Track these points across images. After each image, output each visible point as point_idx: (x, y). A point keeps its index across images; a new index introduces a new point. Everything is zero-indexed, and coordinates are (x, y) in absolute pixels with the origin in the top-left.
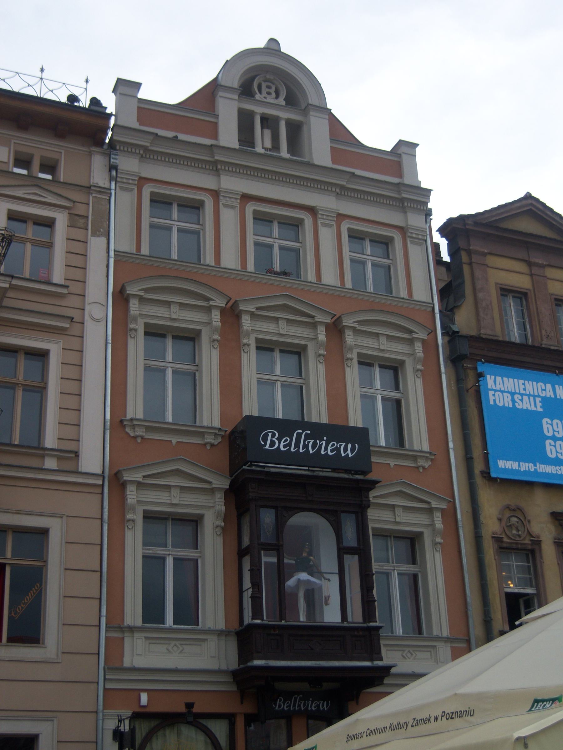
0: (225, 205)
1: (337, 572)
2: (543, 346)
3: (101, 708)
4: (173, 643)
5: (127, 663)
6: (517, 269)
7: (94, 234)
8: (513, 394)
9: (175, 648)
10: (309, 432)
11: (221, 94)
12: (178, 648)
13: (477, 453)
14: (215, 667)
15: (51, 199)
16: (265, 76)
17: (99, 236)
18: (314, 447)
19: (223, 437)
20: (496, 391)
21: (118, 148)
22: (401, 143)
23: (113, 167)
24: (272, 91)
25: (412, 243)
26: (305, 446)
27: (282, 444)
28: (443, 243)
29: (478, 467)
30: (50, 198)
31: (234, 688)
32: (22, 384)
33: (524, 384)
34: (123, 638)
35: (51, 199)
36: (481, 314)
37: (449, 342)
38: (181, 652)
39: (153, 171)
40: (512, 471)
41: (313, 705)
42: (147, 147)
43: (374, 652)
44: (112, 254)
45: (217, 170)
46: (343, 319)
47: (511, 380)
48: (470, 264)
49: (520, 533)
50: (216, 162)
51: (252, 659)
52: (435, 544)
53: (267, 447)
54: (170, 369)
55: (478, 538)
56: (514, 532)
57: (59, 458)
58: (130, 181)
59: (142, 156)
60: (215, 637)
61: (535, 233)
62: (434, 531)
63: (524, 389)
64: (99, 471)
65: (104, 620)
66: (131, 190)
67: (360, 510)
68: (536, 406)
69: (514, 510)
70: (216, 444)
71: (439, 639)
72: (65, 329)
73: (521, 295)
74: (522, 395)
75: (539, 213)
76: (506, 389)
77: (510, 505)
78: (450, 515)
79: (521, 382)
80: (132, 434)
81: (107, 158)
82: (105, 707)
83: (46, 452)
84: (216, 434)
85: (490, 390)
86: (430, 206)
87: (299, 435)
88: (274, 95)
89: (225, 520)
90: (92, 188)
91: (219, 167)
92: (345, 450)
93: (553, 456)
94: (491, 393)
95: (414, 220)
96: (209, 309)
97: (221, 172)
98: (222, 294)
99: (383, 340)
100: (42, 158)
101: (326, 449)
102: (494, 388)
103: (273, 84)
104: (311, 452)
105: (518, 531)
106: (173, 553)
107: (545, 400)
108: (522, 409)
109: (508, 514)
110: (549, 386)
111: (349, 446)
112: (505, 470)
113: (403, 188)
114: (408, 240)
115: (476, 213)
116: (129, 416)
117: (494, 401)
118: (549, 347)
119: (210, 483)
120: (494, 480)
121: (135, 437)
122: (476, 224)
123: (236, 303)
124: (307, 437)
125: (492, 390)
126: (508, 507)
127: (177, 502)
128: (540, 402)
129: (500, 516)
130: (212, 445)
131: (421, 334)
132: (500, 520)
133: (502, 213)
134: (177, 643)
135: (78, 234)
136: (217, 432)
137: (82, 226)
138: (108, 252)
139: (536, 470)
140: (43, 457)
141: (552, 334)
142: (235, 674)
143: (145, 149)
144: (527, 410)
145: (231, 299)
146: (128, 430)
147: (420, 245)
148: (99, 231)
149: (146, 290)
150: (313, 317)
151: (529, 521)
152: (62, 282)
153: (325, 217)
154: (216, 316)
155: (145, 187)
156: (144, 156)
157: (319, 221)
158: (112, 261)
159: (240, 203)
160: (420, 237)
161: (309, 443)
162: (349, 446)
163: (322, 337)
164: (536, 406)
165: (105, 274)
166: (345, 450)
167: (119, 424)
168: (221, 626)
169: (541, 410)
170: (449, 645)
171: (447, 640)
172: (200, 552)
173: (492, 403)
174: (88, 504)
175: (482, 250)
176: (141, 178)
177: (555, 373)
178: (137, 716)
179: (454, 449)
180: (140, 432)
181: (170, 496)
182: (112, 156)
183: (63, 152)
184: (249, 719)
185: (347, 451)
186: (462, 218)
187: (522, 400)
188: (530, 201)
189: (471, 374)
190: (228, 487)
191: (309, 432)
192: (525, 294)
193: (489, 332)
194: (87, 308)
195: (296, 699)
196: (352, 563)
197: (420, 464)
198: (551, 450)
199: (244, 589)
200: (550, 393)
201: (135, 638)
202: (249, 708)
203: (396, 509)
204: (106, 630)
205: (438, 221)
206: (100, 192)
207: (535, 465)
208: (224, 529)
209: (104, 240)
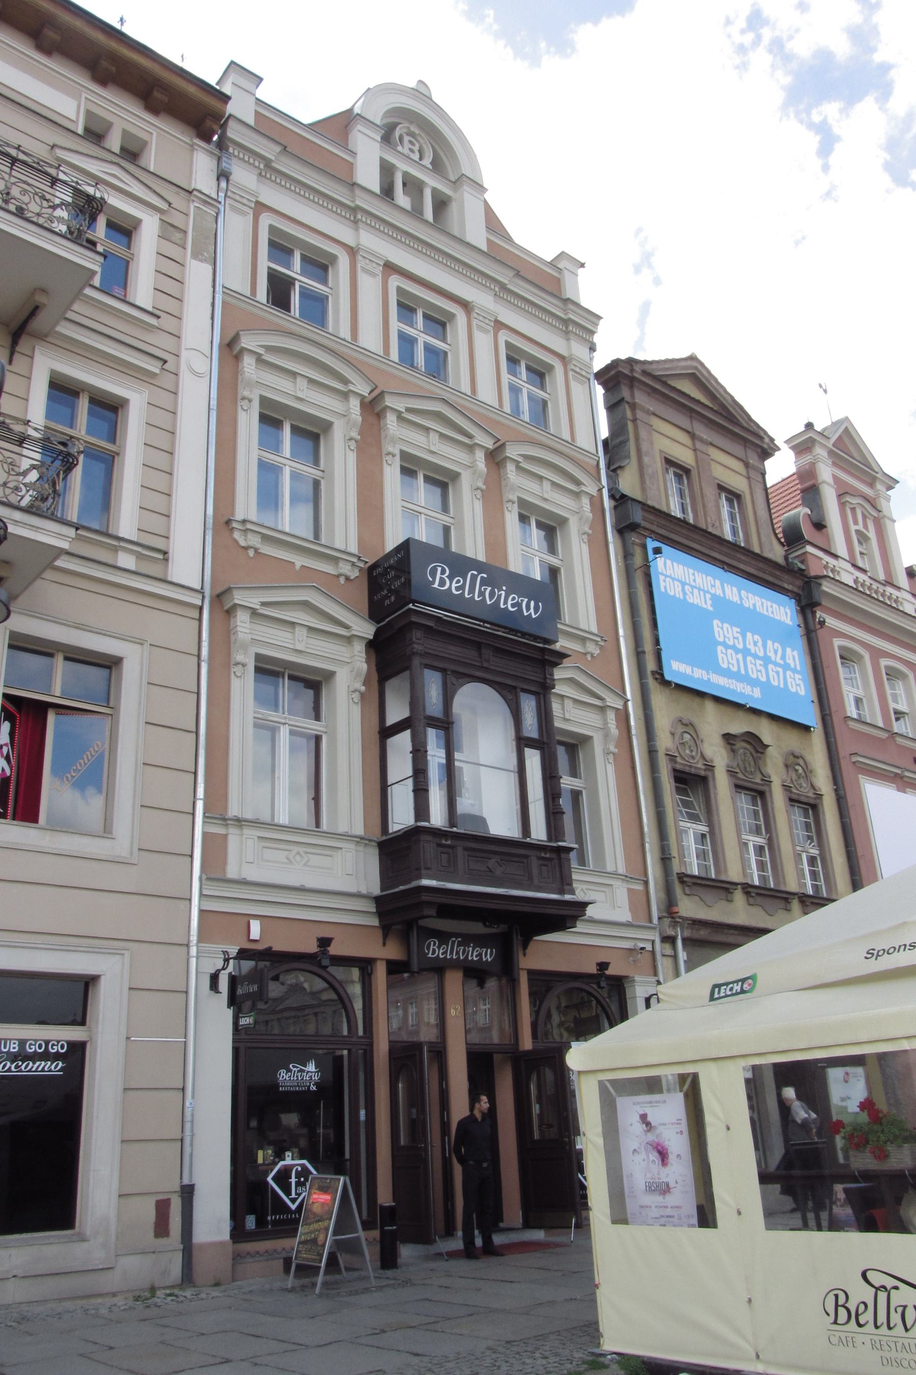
0: (365, 270)
1: (516, 770)
3: (194, 938)
4: (296, 849)
5: (232, 872)
6: (681, 440)
7: (195, 256)
8: (683, 584)
9: (298, 858)
10: (485, 576)
11: (359, 127)
12: (301, 856)
13: (648, 646)
14: (353, 889)
15: (137, 189)
17: (201, 261)
18: (492, 595)
19: (361, 569)
20: (666, 576)
21: (231, 150)
22: (562, 255)
23: (223, 175)
24: (416, 148)
25: (575, 378)
26: (482, 594)
27: (454, 585)
29: (651, 665)
30: (135, 187)
31: (375, 922)
32: (86, 442)
33: (694, 574)
34: (226, 836)
35: (137, 189)
36: (647, 482)
37: (615, 507)
38: (305, 865)
39: (272, 196)
40: (684, 675)
41: (475, 954)
42: (271, 161)
43: (564, 883)
44: (219, 288)
45: (356, 222)
46: (507, 447)
47: (681, 567)
48: (634, 420)
49: (694, 754)
50: (355, 210)
51: (419, 877)
52: (607, 753)
53: (436, 585)
54: (287, 467)
55: (652, 752)
56: (688, 752)
57: (139, 556)
58: (245, 201)
59: (260, 174)
60: (352, 846)
62: (606, 736)
63: (694, 581)
64: (197, 586)
65: (200, 805)
66: (244, 214)
67: (543, 691)
68: (706, 603)
69: (686, 725)
70: (352, 578)
71: (615, 875)
72: (153, 375)
73: (682, 471)
74: (692, 587)
76: (678, 576)
78: (623, 717)
79: (691, 571)
80: (243, 543)
81: (215, 162)
82: (200, 940)
83: (123, 544)
84: (353, 564)
87: (474, 578)
89: (366, 683)
90: (195, 193)
91: (359, 217)
92: (528, 608)
93: (725, 666)
94: (662, 578)
95: (578, 350)
96: (345, 395)
97: (361, 225)
98: (367, 378)
99: (547, 486)
100: (125, 134)
101: (506, 602)
103: (417, 141)
104: (489, 603)
105: (692, 751)
106: (290, 723)
107: (714, 597)
108: (693, 604)
109: (680, 729)
110: (718, 582)
111: (532, 603)
112: (678, 673)
113: (570, 306)
114: (571, 373)
116: (239, 515)
117: (665, 588)
119: (347, 627)
121: (246, 548)
122: (645, 373)
123: (382, 393)
124: (484, 582)
127: (303, 649)
129: (673, 730)
130: (347, 579)
132: (673, 734)
133: (668, 369)
134: (302, 849)
135: (172, 250)
136: (355, 560)
137: (178, 242)
138: (214, 287)
139: (709, 679)
140: (115, 549)
142: (378, 900)
143: (268, 163)
144: (697, 606)
145: (376, 387)
146: (237, 535)
147: (582, 383)
148: (203, 255)
149: (269, 349)
150: (470, 437)
151: (702, 741)
152: (150, 309)
153: (481, 318)
154: (355, 405)
155: (261, 217)
156: (263, 174)
157: (475, 323)
158: (219, 298)
159: (383, 272)
160: (584, 373)
161: (485, 589)
162: (532, 603)
163: (481, 465)
164: (706, 603)
165: (209, 316)
166: (528, 608)
167: (223, 524)
168: (359, 830)
169: (711, 609)
170: (625, 885)
171: (626, 878)
172: (326, 727)
173: (663, 590)
174: (178, 631)
176: (258, 203)
177: (723, 568)
178: (243, 954)
179: (625, 637)
180: (254, 540)
181: (294, 639)
182: (224, 159)
183: (155, 134)
184: (394, 968)
185: (531, 610)
186: (631, 362)
187: (692, 593)
188: (695, 364)
189: (638, 551)
190: (371, 637)
191: (485, 576)
192: (687, 471)
194: (184, 355)
195: (453, 942)
196: (533, 759)
197: (589, 650)
198: (726, 658)
199: (389, 783)
200: (719, 592)
201: (245, 837)
202: (393, 951)
203: (566, 701)
204: (204, 822)
205: (600, 362)
206: (205, 202)
207: (708, 674)
208: (363, 696)
209: (210, 268)
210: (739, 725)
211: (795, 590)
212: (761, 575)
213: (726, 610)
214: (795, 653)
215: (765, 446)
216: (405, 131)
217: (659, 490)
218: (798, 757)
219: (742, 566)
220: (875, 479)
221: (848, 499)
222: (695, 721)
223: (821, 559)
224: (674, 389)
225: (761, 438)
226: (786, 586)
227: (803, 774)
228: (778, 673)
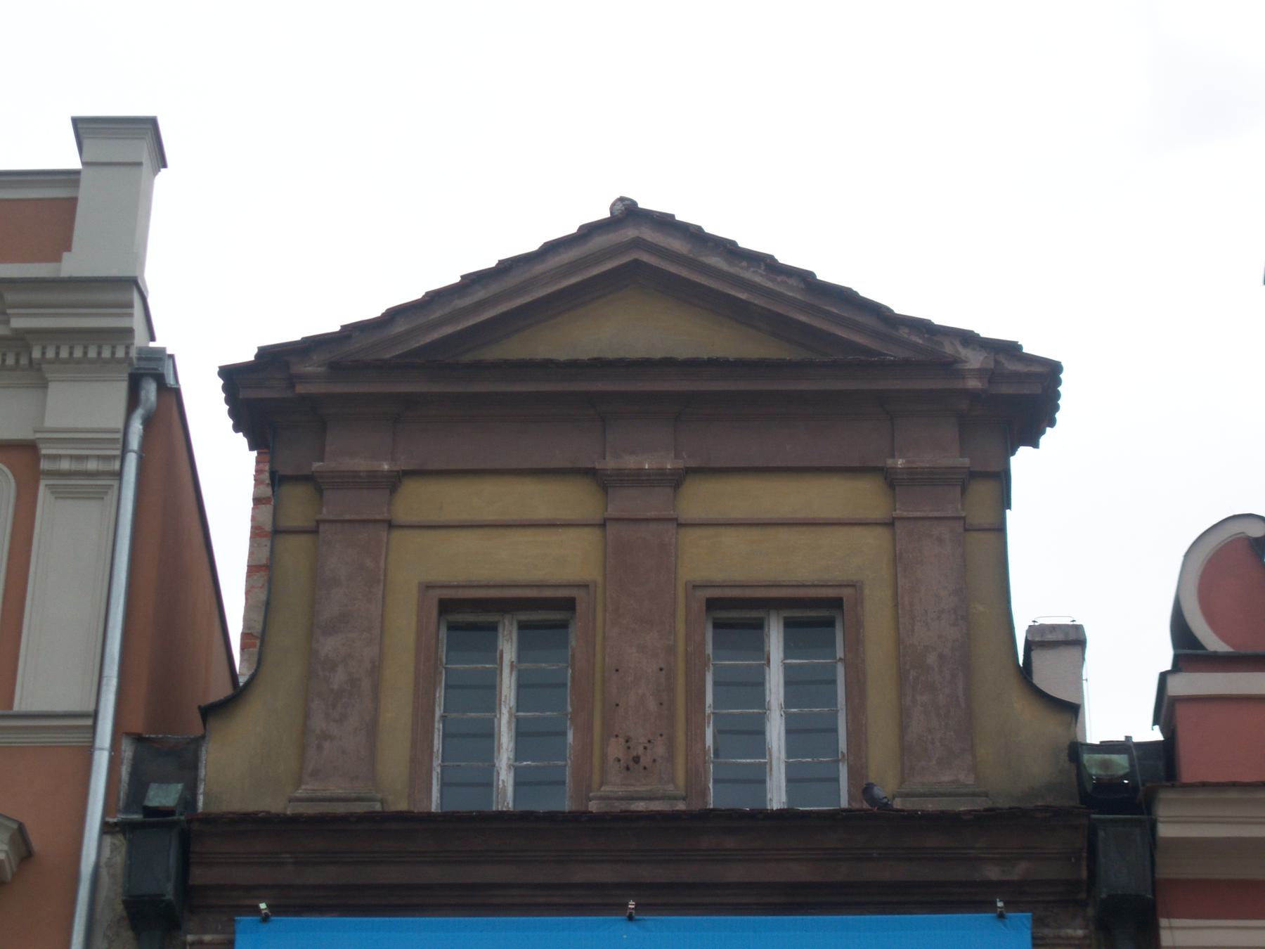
2: (594, 807)
6: (543, 513)
28: (227, 470)
36: (318, 723)
61: (682, 353)
75: (673, 269)
115: (345, 328)
118: (619, 806)
141: (660, 750)
175: (361, 464)
188: (630, 233)
193: (337, 787)
215: (973, 384)
217: (372, 729)
219: (736, 873)
225: (949, 366)
226: (993, 873)
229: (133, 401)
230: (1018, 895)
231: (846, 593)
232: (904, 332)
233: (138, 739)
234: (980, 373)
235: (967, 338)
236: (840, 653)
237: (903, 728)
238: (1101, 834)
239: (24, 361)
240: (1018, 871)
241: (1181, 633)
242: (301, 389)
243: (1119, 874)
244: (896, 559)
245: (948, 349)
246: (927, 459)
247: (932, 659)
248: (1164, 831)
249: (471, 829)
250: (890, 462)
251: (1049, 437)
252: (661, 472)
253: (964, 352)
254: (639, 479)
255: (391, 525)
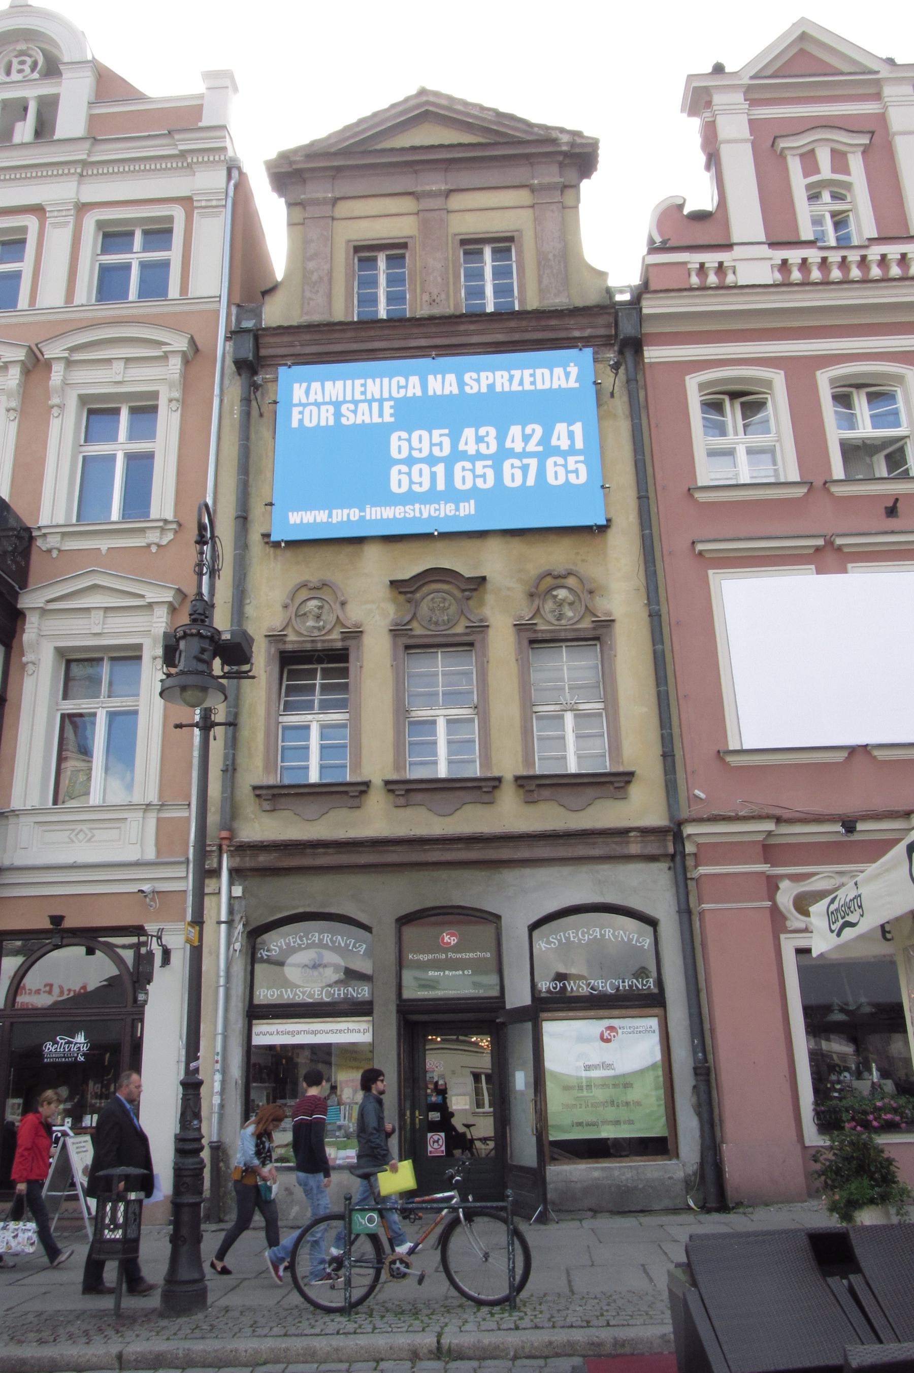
16: (15, 50)
36: (308, 294)
74: (356, 403)
75: (442, 112)
77: (310, 582)
85: (296, 405)
86: (230, 153)
88: (27, 70)
102: (304, 400)
103: (30, 56)
120: (277, 545)
125: (300, 404)
126: (304, 585)
128: (391, 407)
131: (176, 345)
132: (286, 607)
141: (443, 296)
151: (343, 604)
173: (295, 424)
175: (320, 195)
188: (424, 99)
207: (362, 509)
210: (411, 565)
211: (602, 332)
212: (516, 337)
213: (412, 414)
214: (578, 428)
216: (15, 53)
217: (329, 296)
218: (564, 577)
219: (475, 339)
220: (878, 83)
221: (782, 145)
222: (334, 576)
223: (685, 263)
224: (383, 151)
225: (554, 141)
226: (577, 334)
227: (571, 598)
228: (525, 469)
229: (229, 177)
230: (586, 342)
231: (515, 234)
232: (536, 129)
233: (238, 306)
234: (567, 143)
235: (562, 130)
236: (514, 258)
237: (540, 282)
238: (620, 314)
239: (185, 165)
240: (587, 333)
241: (651, 241)
242: (294, 167)
243: (627, 329)
244: (535, 219)
245: (554, 134)
246: (546, 180)
247: (550, 256)
248: (645, 311)
249: (369, 324)
250: (532, 182)
251: (595, 175)
252: (440, 190)
253: (560, 136)
254: (431, 195)
255: (333, 219)
